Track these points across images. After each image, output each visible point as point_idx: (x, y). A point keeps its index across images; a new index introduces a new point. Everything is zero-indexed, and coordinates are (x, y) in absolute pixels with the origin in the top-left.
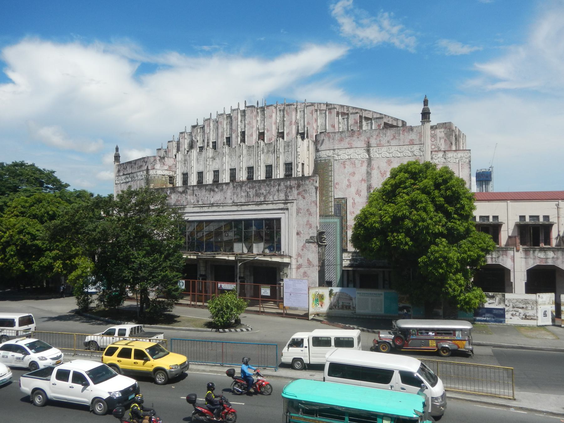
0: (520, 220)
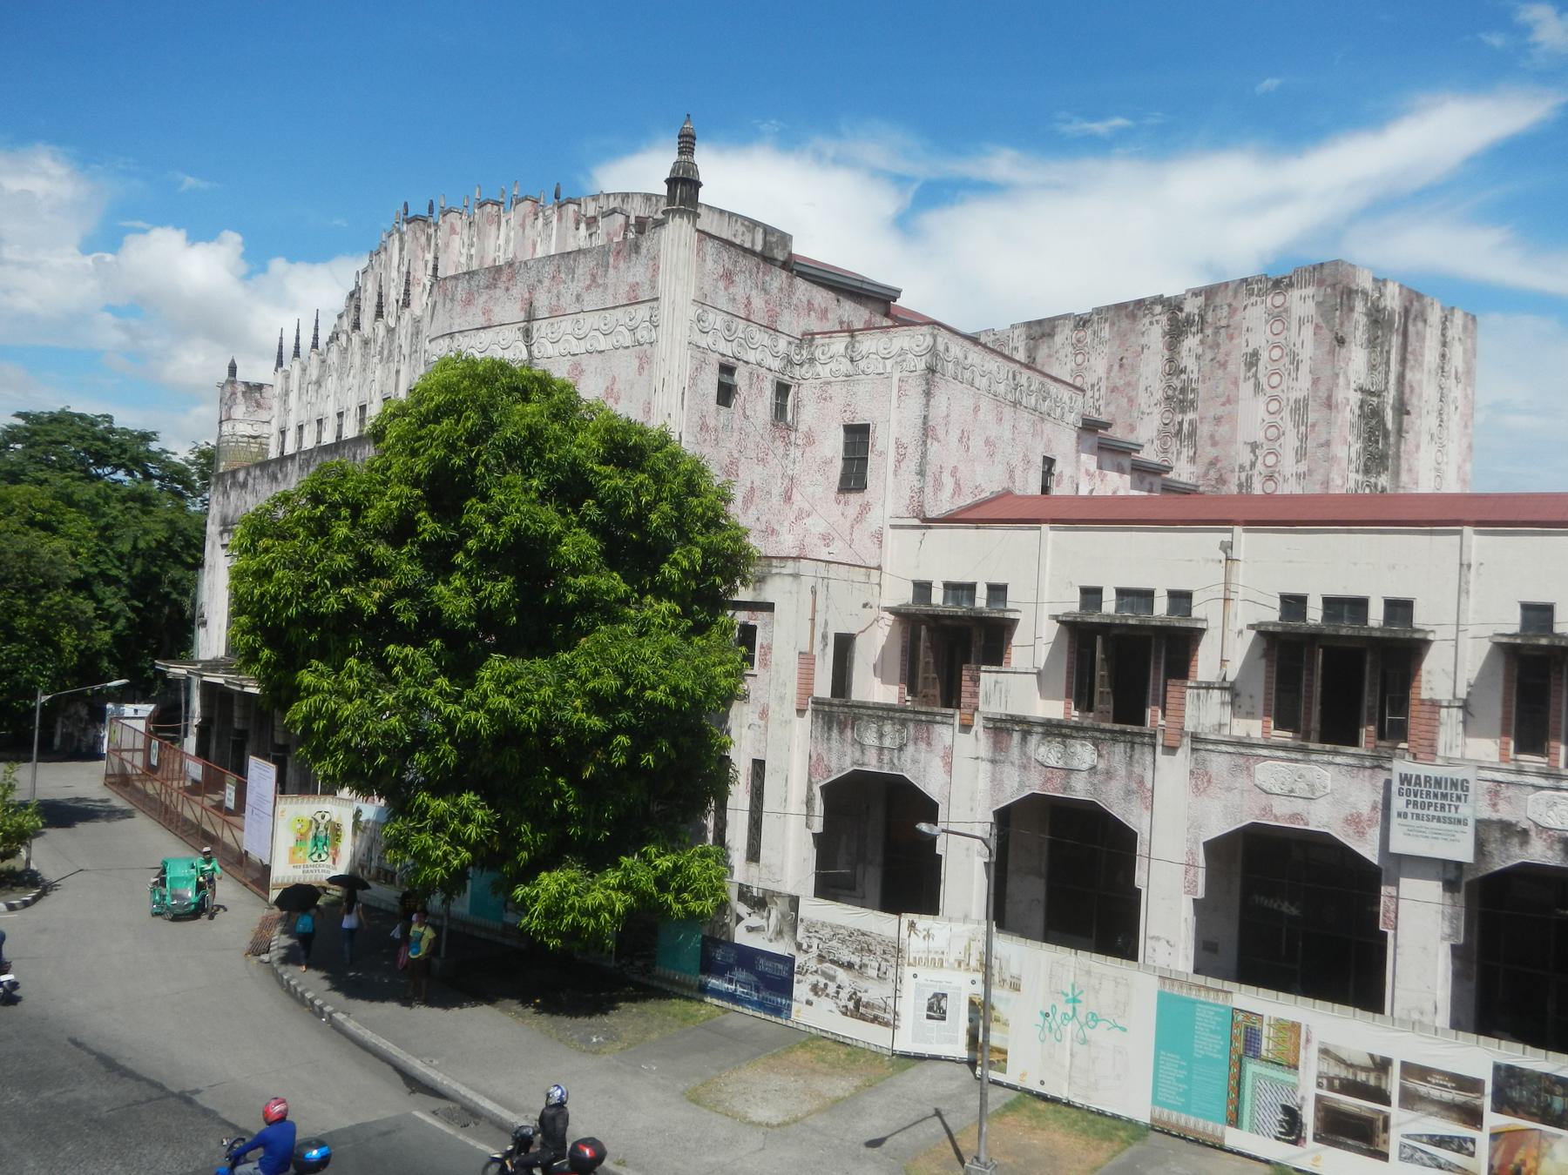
0: (1083, 607)
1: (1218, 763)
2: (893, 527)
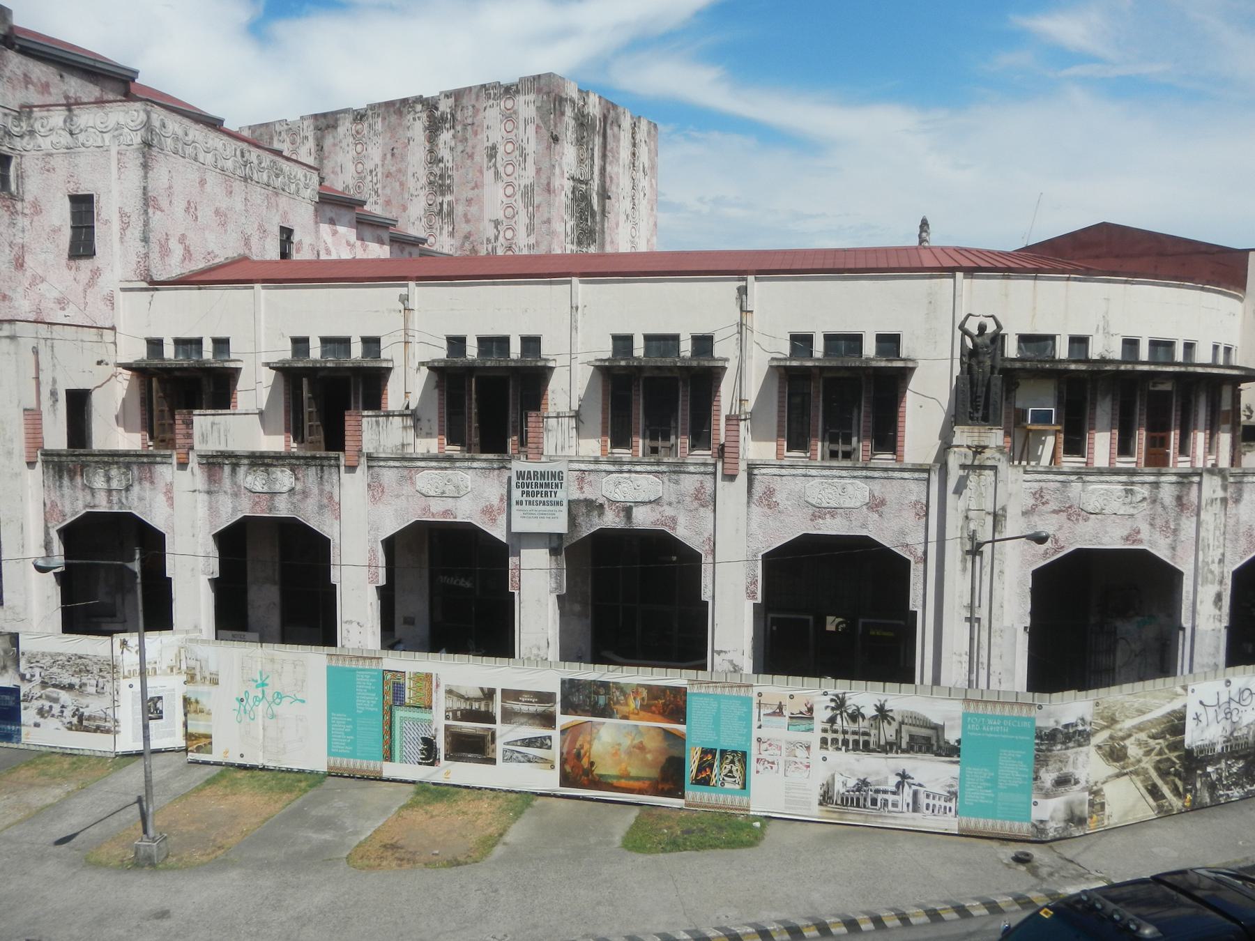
1: (389, 476)
2: (124, 290)
